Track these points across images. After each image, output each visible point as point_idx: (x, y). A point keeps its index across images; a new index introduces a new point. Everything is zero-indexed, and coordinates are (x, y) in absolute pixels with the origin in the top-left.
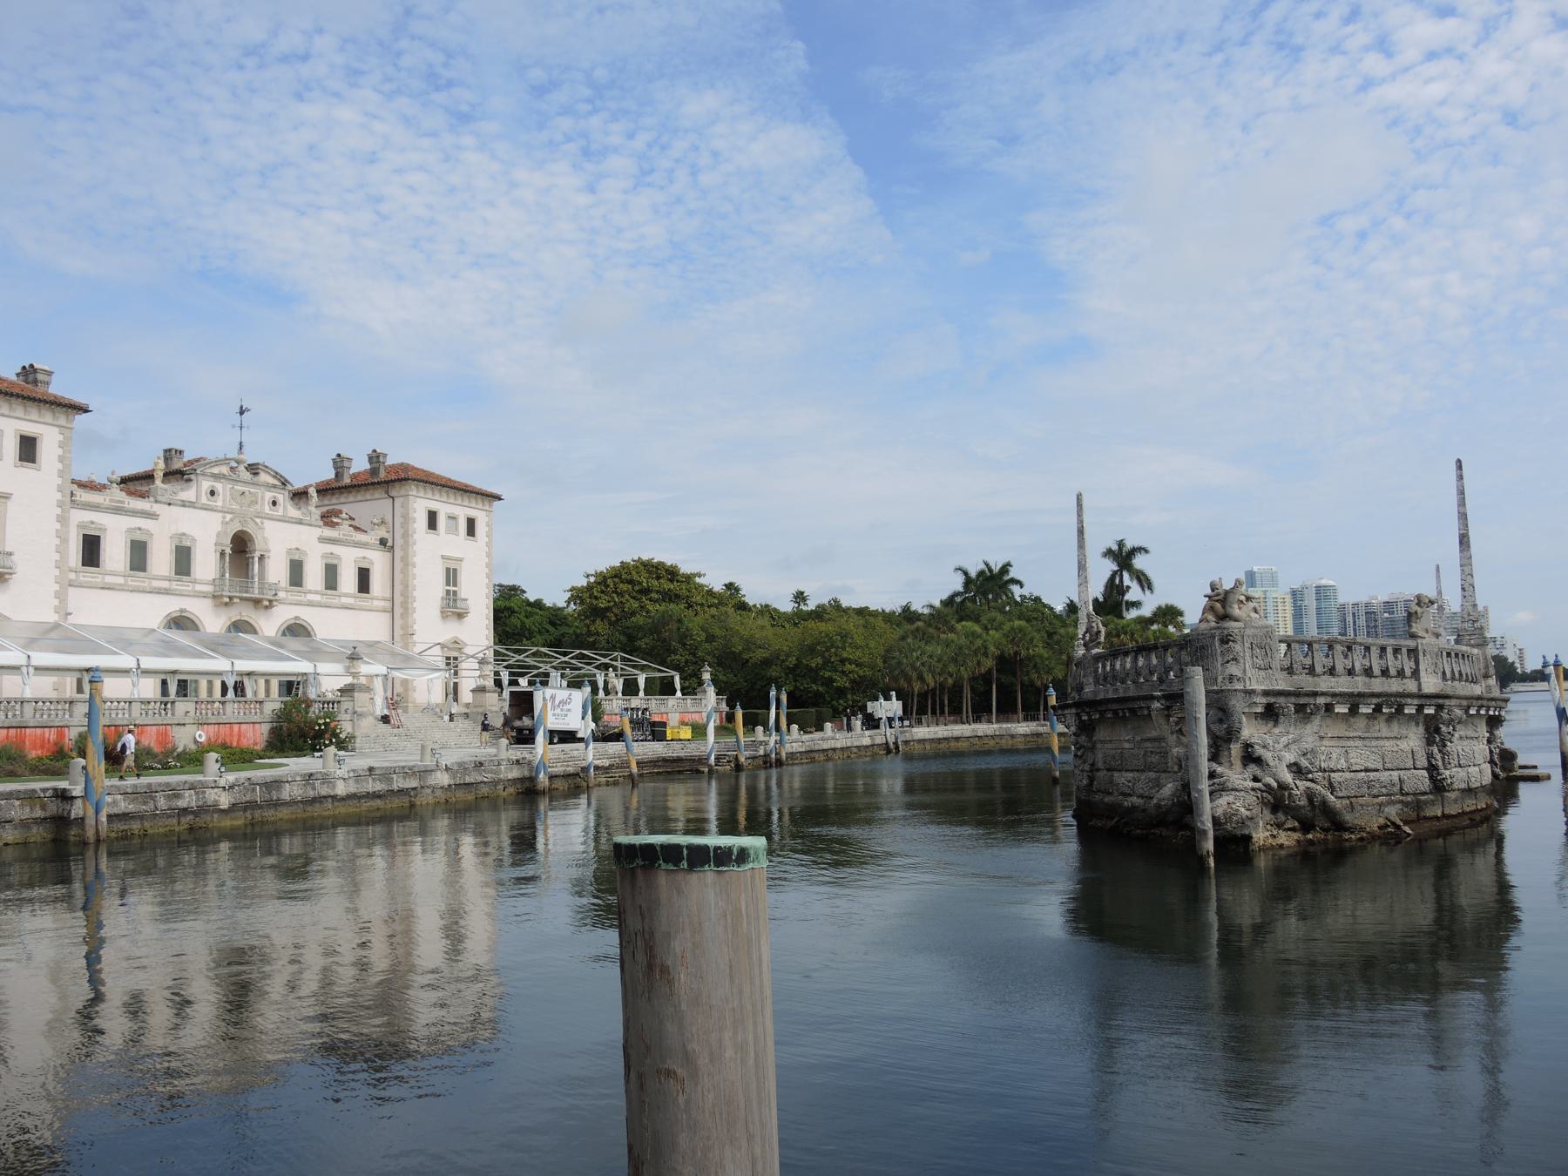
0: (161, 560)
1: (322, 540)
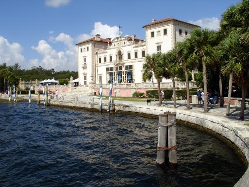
0: (108, 59)
1: (134, 47)
